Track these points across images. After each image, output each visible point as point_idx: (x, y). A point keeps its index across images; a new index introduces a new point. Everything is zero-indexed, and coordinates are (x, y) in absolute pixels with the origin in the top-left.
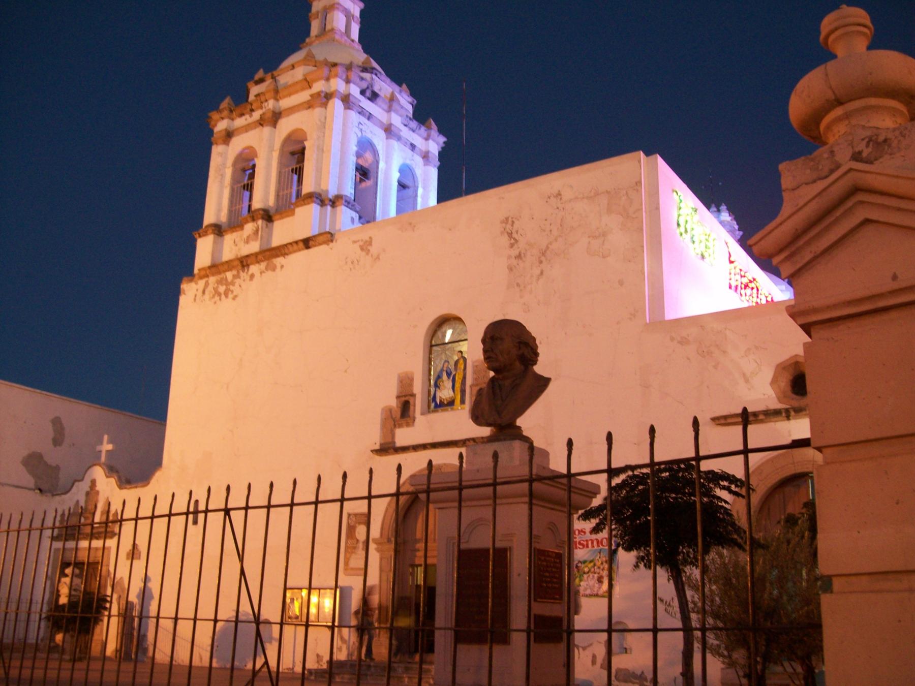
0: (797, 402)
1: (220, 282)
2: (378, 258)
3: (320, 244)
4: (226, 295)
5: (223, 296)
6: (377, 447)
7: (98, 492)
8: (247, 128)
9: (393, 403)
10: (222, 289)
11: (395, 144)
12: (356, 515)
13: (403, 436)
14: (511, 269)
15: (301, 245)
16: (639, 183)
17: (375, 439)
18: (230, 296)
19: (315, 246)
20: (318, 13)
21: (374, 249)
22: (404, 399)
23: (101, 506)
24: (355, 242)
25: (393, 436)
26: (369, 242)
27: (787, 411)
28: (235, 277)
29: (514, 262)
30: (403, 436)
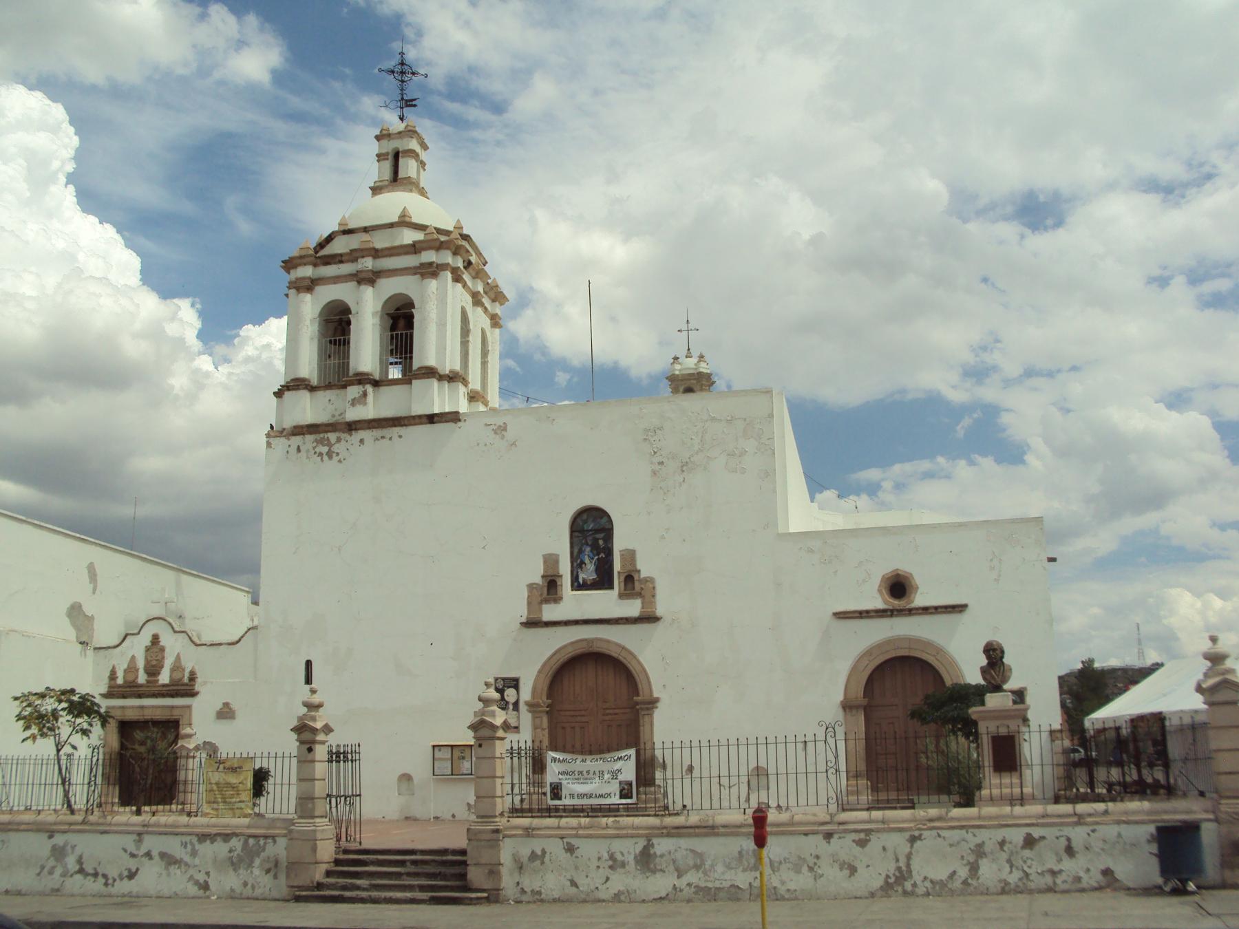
0: (896, 603)
1: (320, 442)
2: (514, 444)
4: (330, 457)
5: (326, 458)
6: (524, 620)
7: (163, 650)
8: (336, 280)
9: (538, 580)
10: (325, 449)
11: (479, 309)
12: (504, 679)
13: (550, 612)
14: (654, 473)
15: (425, 420)
16: (771, 416)
17: (521, 611)
18: (335, 458)
20: (387, 154)
21: (510, 434)
23: (168, 663)
25: (541, 610)
26: (504, 428)
27: (892, 611)
28: (339, 440)
29: (658, 467)
30: (550, 612)
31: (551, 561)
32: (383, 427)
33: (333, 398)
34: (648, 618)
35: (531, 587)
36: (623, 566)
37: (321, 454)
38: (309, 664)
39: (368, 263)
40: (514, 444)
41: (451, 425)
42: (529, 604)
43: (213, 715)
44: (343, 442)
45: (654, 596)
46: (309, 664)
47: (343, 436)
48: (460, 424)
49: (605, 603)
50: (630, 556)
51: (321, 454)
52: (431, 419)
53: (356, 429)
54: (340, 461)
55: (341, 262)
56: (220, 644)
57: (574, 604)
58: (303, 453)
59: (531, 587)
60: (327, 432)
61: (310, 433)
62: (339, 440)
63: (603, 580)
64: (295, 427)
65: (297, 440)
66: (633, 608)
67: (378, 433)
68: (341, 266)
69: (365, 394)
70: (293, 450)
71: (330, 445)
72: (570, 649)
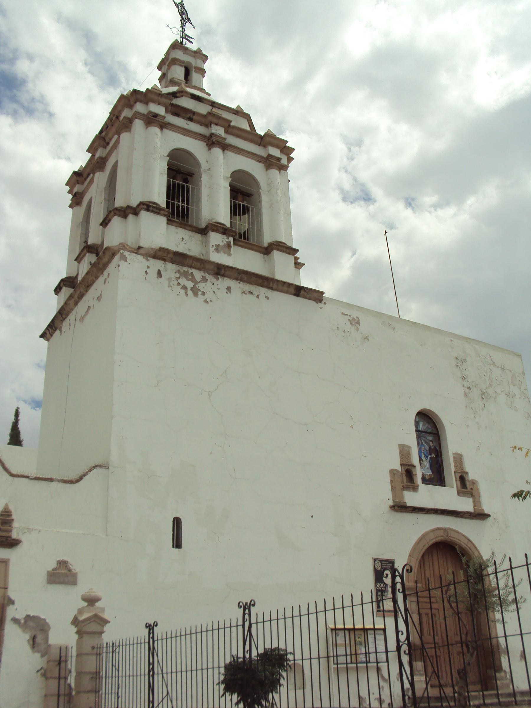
1: (185, 275)
2: (366, 338)
3: (310, 299)
5: (190, 293)
8: (186, 132)
12: (381, 561)
15: (292, 290)
17: (386, 496)
19: (305, 297)
22: (407, 467)
24: (343, 314)
29: (467, 391)
30: (411, 499)
31: (404, 452)
32: (249, 282)
33: (186, 238)
34: (480, 515)
35: (393, 472)
36: (456, 467)
37: (184, 288)
38: (177, 523)
39: (220, 131)
40: (366, 338)
41: (312, 303)
42: (393, 488)
43: (42, 577)
44: (208, 283)
45: (479, 496)
46: (177, 523)
47: (209, 277)
48: (321, 305)
49: (446, 497)
50: (459, 459)
51: (184, 288)
52: (299, 291)
53: (223, 276)
54: (206, 301)
55: (191, 119)
56: (51, 480)
57: (425, 496)
58: (164, 280)
59: (393, 472)
60: (191, 267)
61: (173, 262)
62: (204, 280)
63: (437, 478)
64: (161, 249)
65: (157, 264)
66: (465, 505)
67: (247, 287)
68: (189, 122)
69: (229, 246)
70: (153, 272)
71: (193, 280)
72: (432, 536)
